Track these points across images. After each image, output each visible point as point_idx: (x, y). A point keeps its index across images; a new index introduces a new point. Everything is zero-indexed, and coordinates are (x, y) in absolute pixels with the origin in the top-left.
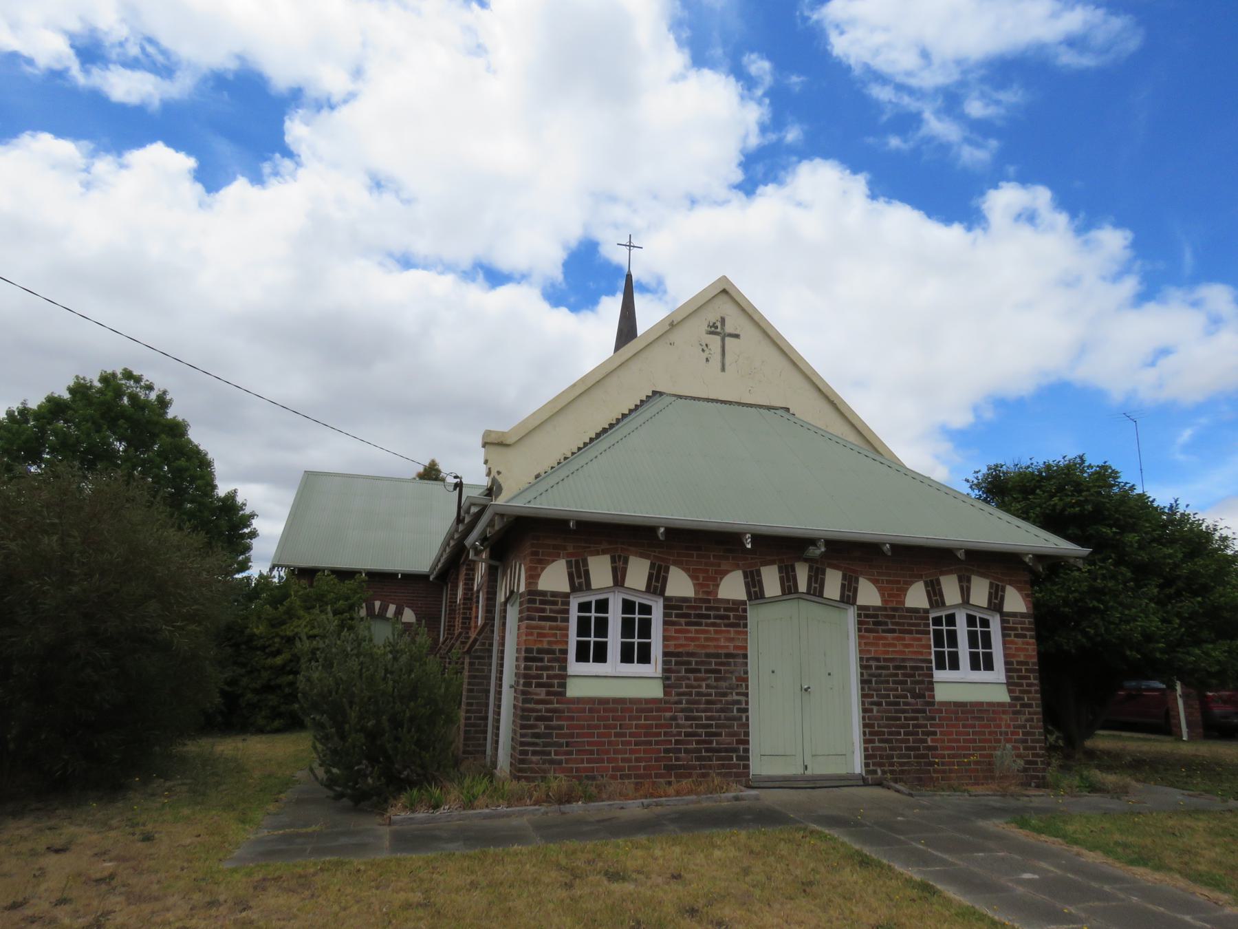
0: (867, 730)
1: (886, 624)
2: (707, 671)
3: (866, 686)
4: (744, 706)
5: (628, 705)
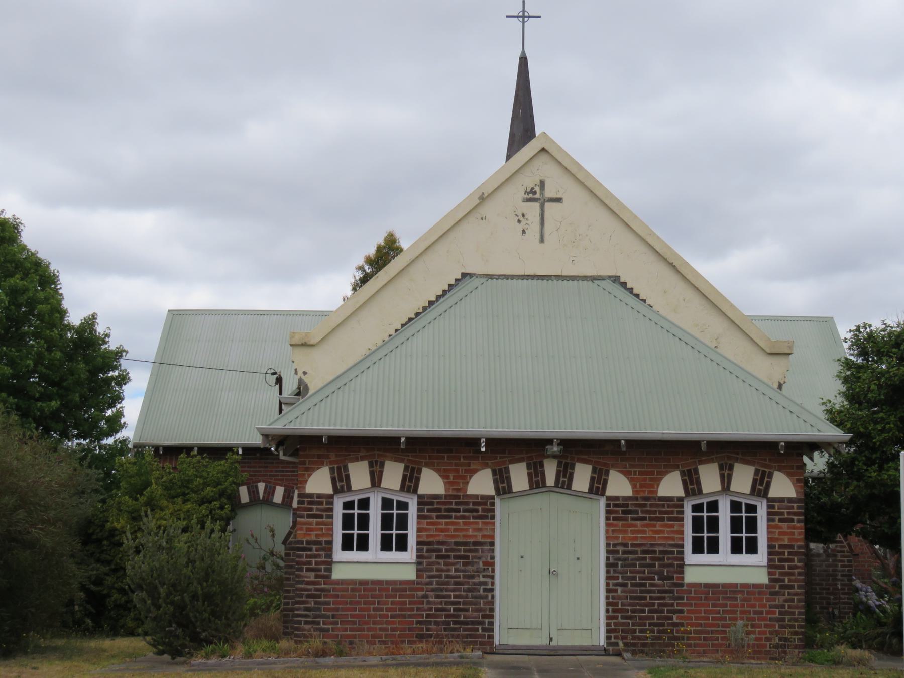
0: (610, 608)
1: (636, 512)
2: (456, 557)
3: (612, 569)
4: (489, 586)
5: (385, 586)
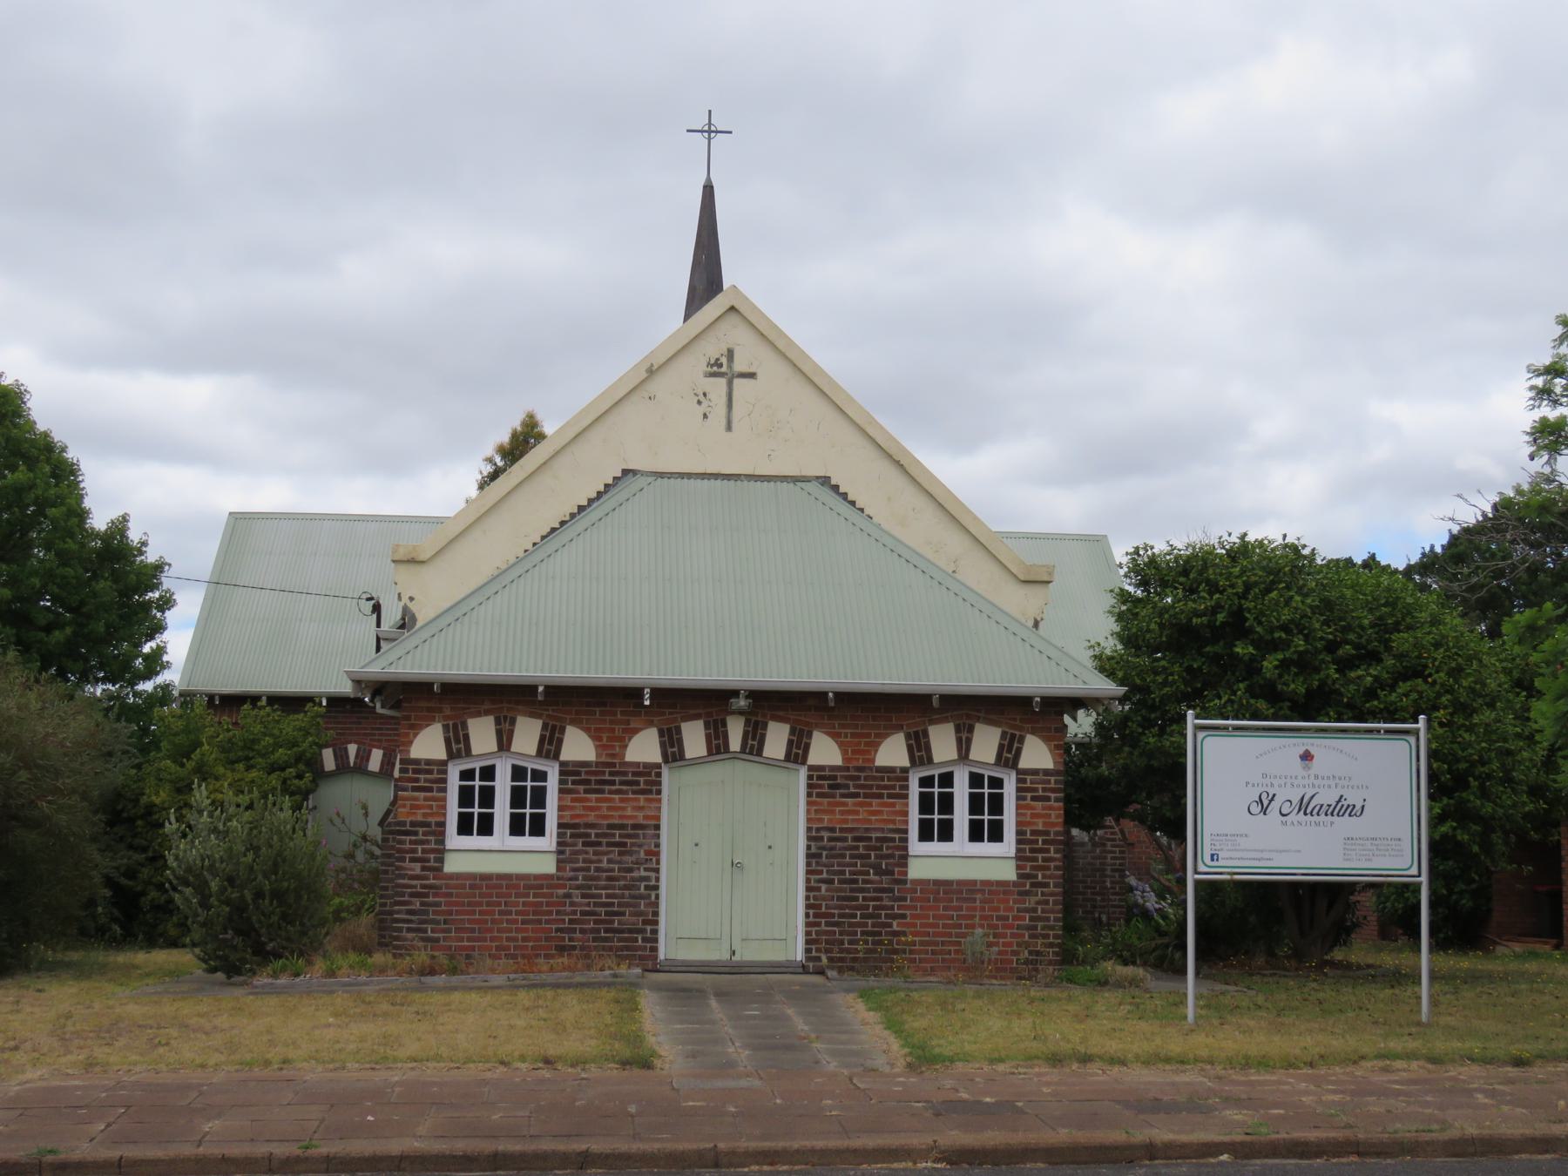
0: (811, 912)
1: (847, 786)
2: (609, 844)
3: (814, 861)
4: (653, 883)
